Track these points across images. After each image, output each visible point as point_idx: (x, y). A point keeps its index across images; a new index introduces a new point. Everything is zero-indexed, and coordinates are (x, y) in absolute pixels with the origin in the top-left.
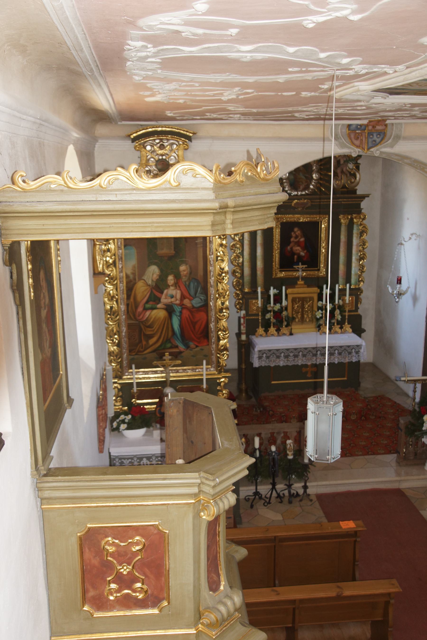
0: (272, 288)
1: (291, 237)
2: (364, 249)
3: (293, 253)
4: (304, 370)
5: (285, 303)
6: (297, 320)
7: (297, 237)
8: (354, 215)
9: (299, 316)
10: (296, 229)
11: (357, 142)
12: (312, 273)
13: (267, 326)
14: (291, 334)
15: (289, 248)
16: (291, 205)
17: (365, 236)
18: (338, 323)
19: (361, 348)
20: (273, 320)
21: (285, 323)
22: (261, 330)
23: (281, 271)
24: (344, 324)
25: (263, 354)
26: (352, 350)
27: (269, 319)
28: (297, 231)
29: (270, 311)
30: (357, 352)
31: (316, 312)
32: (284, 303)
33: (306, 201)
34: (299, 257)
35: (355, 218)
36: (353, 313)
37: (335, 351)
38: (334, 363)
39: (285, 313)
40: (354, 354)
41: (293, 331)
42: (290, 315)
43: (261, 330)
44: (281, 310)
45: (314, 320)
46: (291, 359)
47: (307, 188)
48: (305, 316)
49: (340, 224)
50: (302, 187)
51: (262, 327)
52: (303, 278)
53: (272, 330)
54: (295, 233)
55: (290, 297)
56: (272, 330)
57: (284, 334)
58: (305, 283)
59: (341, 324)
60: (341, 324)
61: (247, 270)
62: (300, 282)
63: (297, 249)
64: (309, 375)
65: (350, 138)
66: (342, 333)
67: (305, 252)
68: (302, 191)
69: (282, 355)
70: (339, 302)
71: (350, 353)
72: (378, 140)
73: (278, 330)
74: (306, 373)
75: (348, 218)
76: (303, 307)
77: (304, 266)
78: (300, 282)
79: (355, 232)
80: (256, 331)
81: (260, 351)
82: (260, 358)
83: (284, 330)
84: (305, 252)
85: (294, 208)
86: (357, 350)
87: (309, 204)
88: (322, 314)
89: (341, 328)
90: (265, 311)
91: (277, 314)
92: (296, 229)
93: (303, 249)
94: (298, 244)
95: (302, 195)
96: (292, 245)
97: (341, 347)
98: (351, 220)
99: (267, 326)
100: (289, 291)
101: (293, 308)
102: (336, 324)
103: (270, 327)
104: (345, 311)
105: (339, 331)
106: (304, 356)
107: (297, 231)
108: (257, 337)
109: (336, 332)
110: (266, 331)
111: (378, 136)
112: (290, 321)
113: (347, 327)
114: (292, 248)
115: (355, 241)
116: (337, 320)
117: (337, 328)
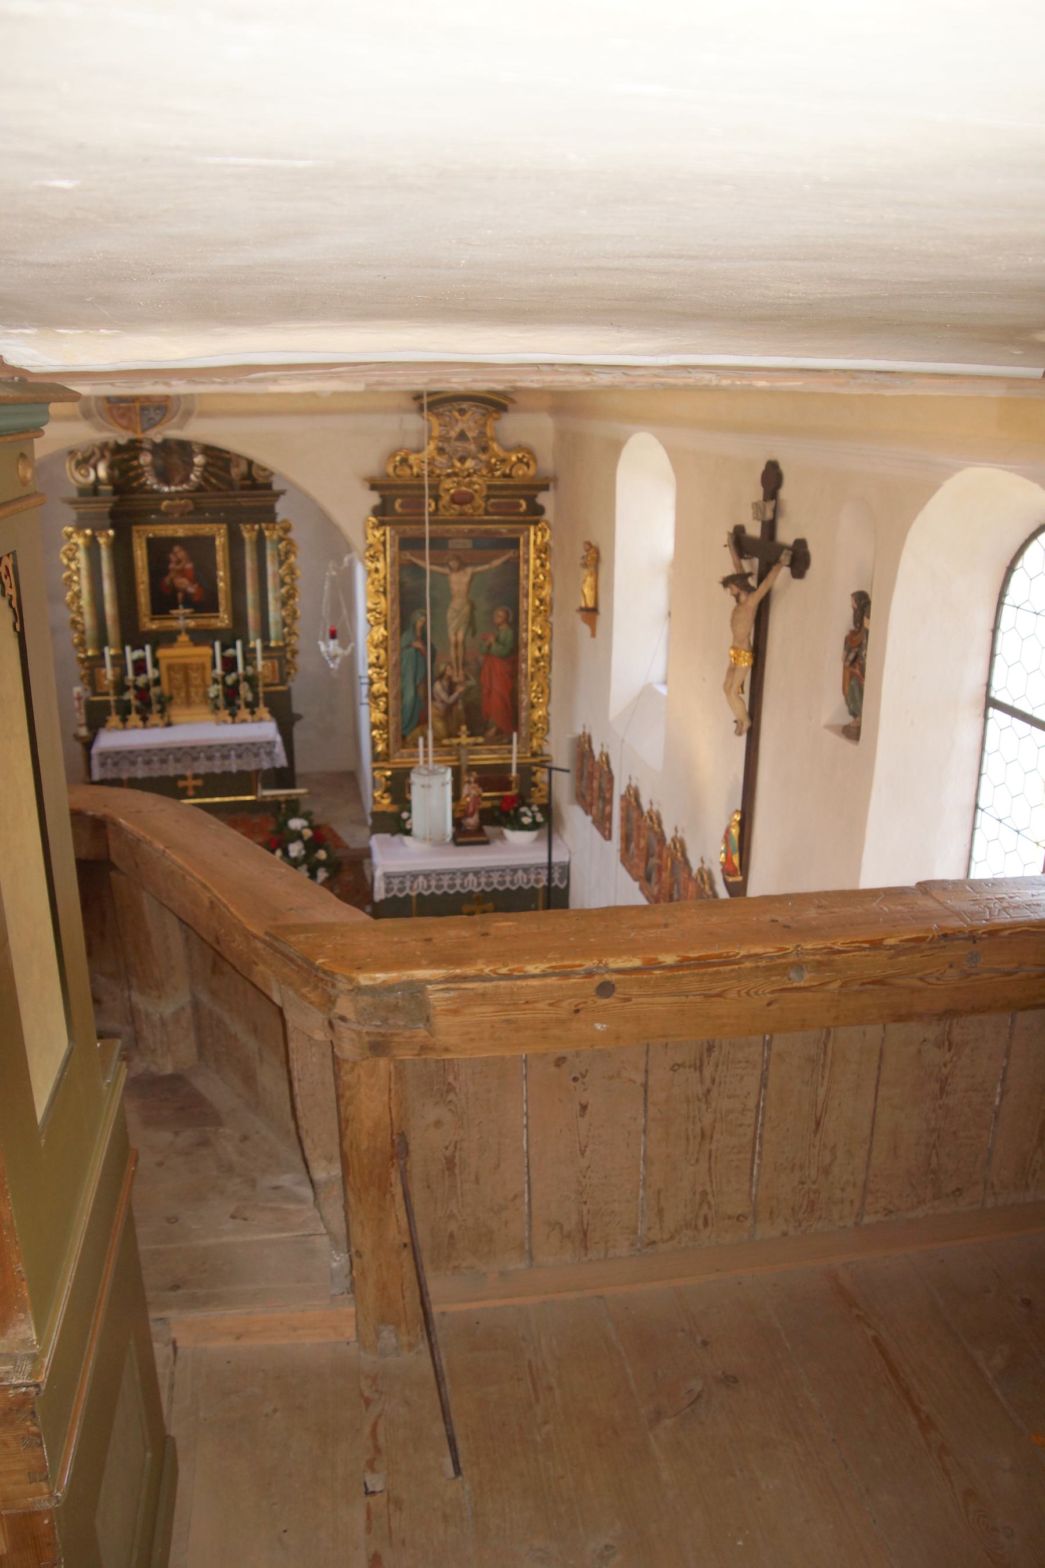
0: (128, 649)
1: (169, 562)
2: (293, 580)
3: (175, 590)
4: (181, 784)
5: (154, 673)
6: (178, 700)
7: (179, 562)
8: (264, 525)
9: (183, 694)
10: (177, 549)
11: (124, 422)
12: (204, 622)
13: (124, 711)
14: (169, 724)
15: (167, 580)
16: (160, 508)
17: (292, 559)
18: (248, 705)
19: (274, 746)
20: (135, 703)
21: (156, 707)
22: (114, 719)
23: (152, 619)
24: (257, 706)
25: (106, 759)
26: (259, 749)
27: (129, 701)
28: (179, 552)
29: (127, 688)
30: (270, 754)
31: (208, 686)
32: (151, 673)
33: (183, 502)
34: (187, 595)
35: (267, 529)
36: (273, 689)
37: (229, 751)
38: (230, 773)
39: (154, 691)
40: (263, 756)
41: (174, 719)
42: (167, 693)
43: (114, 719)
44: (147, 687)
45: (209, 701)
46: (156, 765)
47: (186, 480)
48: (193, 695)
49: (242, 541)
50: (177, 479)
51: (118, 713)
52: (189, 631)
53: (134, 718)
54: (175, 554)
55: (163, 664)
56: (134, 718)
57: (155, 726)
58: (192, 639)
59: (252, 706)
60: (252, 706)
61: (88, 620)
62: (184, 638)
63: (182, 582)
64: (191, 793)
65: (113, 416)
66: (253, 721)
67: (196, 586)
68: (176, 485)
69: (140, 759)
70: (245, 669)
71: (257, 755)
72: (157, 418)
73: (144, 719)
74: (185, 788)
75: (253, 529)
76: (187, 680)
77: (188, 611)
78: (184, 638)
79: (269, 552)
80: (106, 721)
81: (101, 754)
82: (103, 765)
83: (154, 718)
84: (196, 586)
85: (166, 514)
86: (268, 750)
87: (191, 507)
88: (218, 690)
89: (253, 713)
90: (121, 687)
91: (143, 693)
92: (177, 549)
93: (193, 580)
94: (182, 573)
95: (177, 492)
96: (172, 575)
97: (240, 745)
98: (261, 533)
99: (124, 711)
100: (162, 653)
101: (170, 681)
102: (243, 706)
103: (130, 713)
104: (257, 686)
105: (249, 717)
106: (177, 760)
107: (179, 552)
108: (109, 730)
109: (244, 721)
110: (124, 720)
111: (158, 411)
112: (165, 703)
113: (263, 711)
114: (172, 581)
115: (271, 567)
116: (245, 699)
117: (244, 713)
